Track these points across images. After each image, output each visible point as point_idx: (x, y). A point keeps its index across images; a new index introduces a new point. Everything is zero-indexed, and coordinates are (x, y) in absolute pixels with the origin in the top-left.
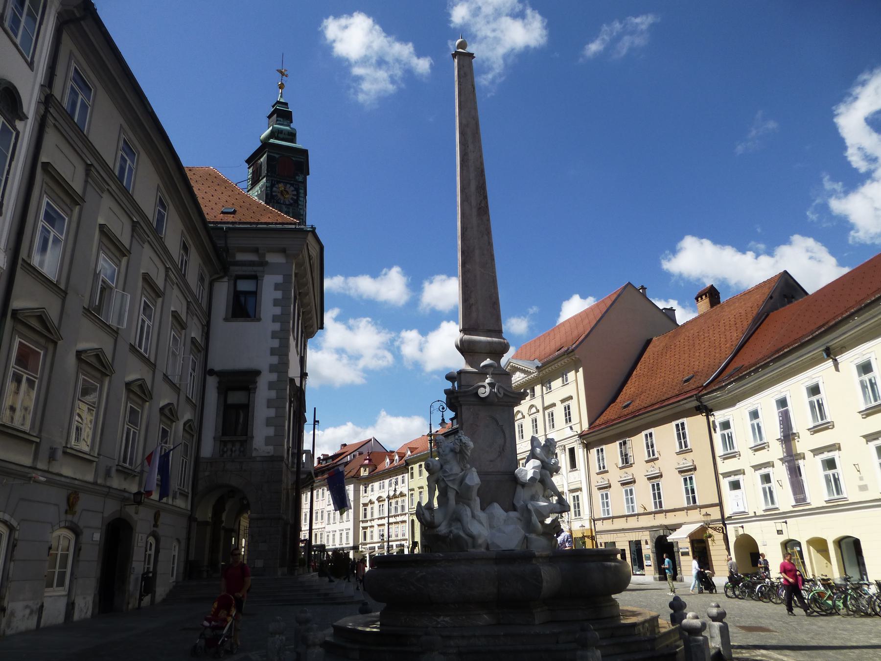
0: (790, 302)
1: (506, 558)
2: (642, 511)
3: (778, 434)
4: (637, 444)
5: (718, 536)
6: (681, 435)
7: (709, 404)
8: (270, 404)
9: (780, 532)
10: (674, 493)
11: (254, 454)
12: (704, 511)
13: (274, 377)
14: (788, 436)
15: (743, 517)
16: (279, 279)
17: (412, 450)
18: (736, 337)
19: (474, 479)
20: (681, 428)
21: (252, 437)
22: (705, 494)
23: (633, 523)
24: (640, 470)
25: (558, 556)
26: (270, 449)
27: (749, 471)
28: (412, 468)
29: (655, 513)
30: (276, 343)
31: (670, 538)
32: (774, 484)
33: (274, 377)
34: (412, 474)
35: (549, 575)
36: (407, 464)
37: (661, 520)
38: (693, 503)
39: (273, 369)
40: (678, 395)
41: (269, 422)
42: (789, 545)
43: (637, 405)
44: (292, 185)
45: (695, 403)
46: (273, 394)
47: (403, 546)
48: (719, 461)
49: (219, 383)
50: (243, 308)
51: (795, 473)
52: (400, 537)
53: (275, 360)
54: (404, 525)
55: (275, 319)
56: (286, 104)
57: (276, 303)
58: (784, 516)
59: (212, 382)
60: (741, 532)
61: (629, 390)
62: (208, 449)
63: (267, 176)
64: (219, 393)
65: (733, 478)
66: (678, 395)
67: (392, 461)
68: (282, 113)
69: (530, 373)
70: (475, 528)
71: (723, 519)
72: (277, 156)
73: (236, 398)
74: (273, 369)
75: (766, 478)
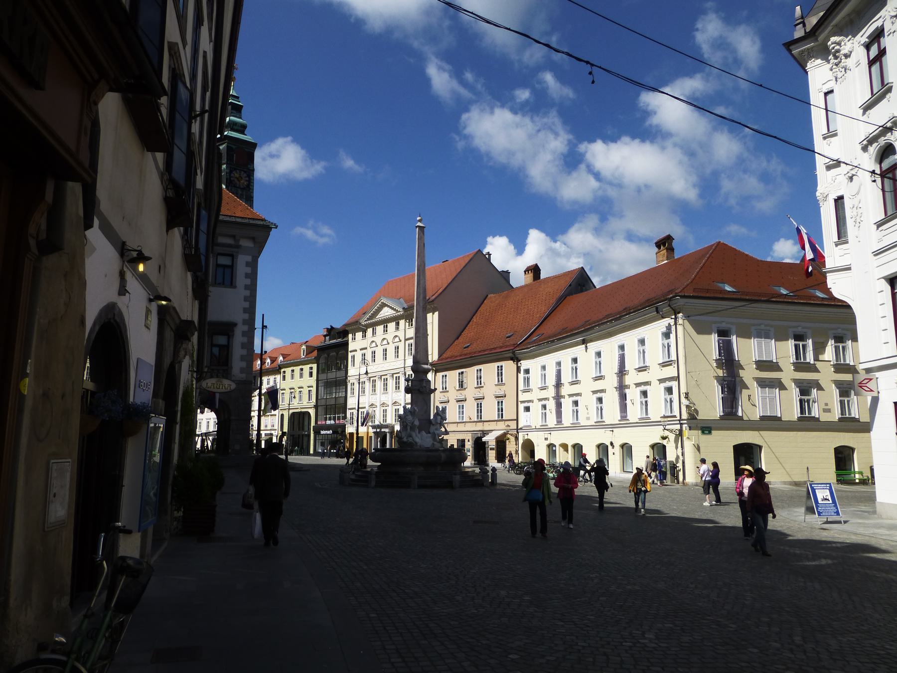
0: (582, 291)
1: (428, 450)
2: (468, 420)
3: (554, 383)
4: (471, 373)
5: (512, 439)
6: (500, 374)
7: (519, 356)
9: (546, 439)
10: (490, 411)
12: (507, 423)
14: (558, 385)
15: (529, 429)
16: (249, 258)
17: (284, 356)
18: (544, 310)
19: (417, 423)
20: (500, 368)
21: (232, 368)
22: (509, 413)
23: (461, 427)
24: (470, 392)
25: (446, 450)
26: (243, 376)
27: (536, 401)
28: (284, 372)
29: (476, 422)
30: (247, 305)
31: (484, 439)
32: (547, 411)
33: (246, 328)
34: (284, 377)
35: (443, 455)
36: (280, 367)
37: (480, 427)
38: (501, 418)
39: (245, 322)
40: (501, 347)
42: (551, 446)
43: (475, 347)
44: (245, 172)
45: (511, 355)
47: (272, 434)
48: (520, 393)
51: (559, 405)
52: (269, 428)
53: (246, 316)
54: (273, 417)
55: (246, 287)
56: (238, 98)
57: (247, 276)
58: (550, 430)
60: (526, 437)
61: (469, 333)
63: (227, 164)
65: (526, 405)
66: (501, 347)
67: (263, 363)
69: (397, 311)
70: (417, 440)
71: (517, 429)
72: (234, 147)
75: (544, 407)
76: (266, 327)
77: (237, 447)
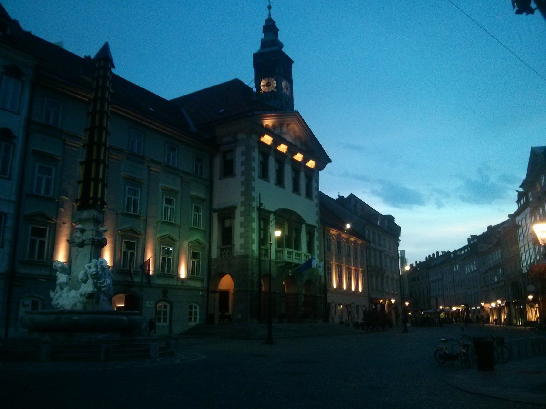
8: (242, 225)
11: (235, 255)
13: (243, 209)
21: (234, 245)
30: (243, 188)
33: (243, 209)
39: (242, 204)
41: (242, 236)
46: (243, 219)
49: (218, 216)
50: (228, 170)
53: (243, 198)
55: (243, 173)
57: (243, 164)
59: (215, 216)
62: (215, 253)
64: (219, 222)
68: (270, 28)
73: (227, 223)
74: (242, 204)
76: (262, 204)
77: (239, 316)
